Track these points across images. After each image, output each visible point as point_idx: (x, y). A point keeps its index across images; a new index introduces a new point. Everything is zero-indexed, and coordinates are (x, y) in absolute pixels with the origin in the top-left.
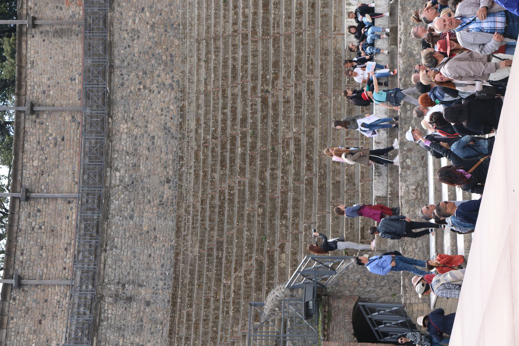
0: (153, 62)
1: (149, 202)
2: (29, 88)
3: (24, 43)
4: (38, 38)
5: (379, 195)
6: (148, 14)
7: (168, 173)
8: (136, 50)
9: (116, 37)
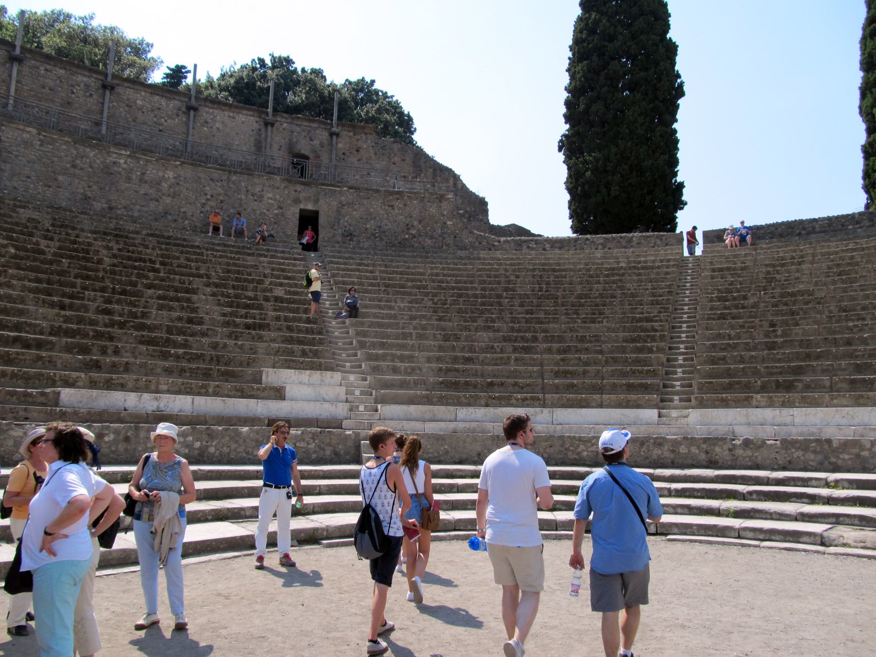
0: (232, 211)
1: (90, 187)
2: (211, 110)
3: (252, 113)
4: (256, 126)
5: (62, 396)
6: (276, 212)
7: (120, 209)
8: (243, 197)
9: (256, 180)
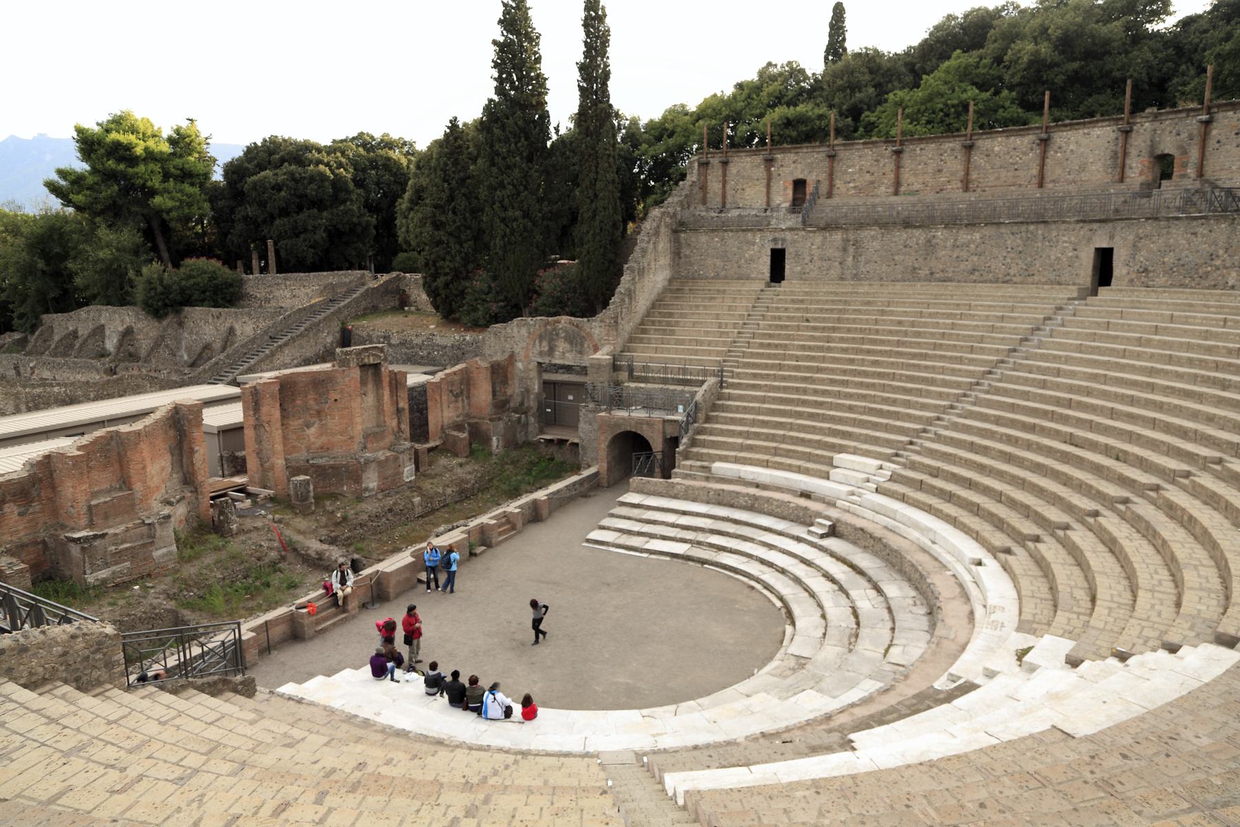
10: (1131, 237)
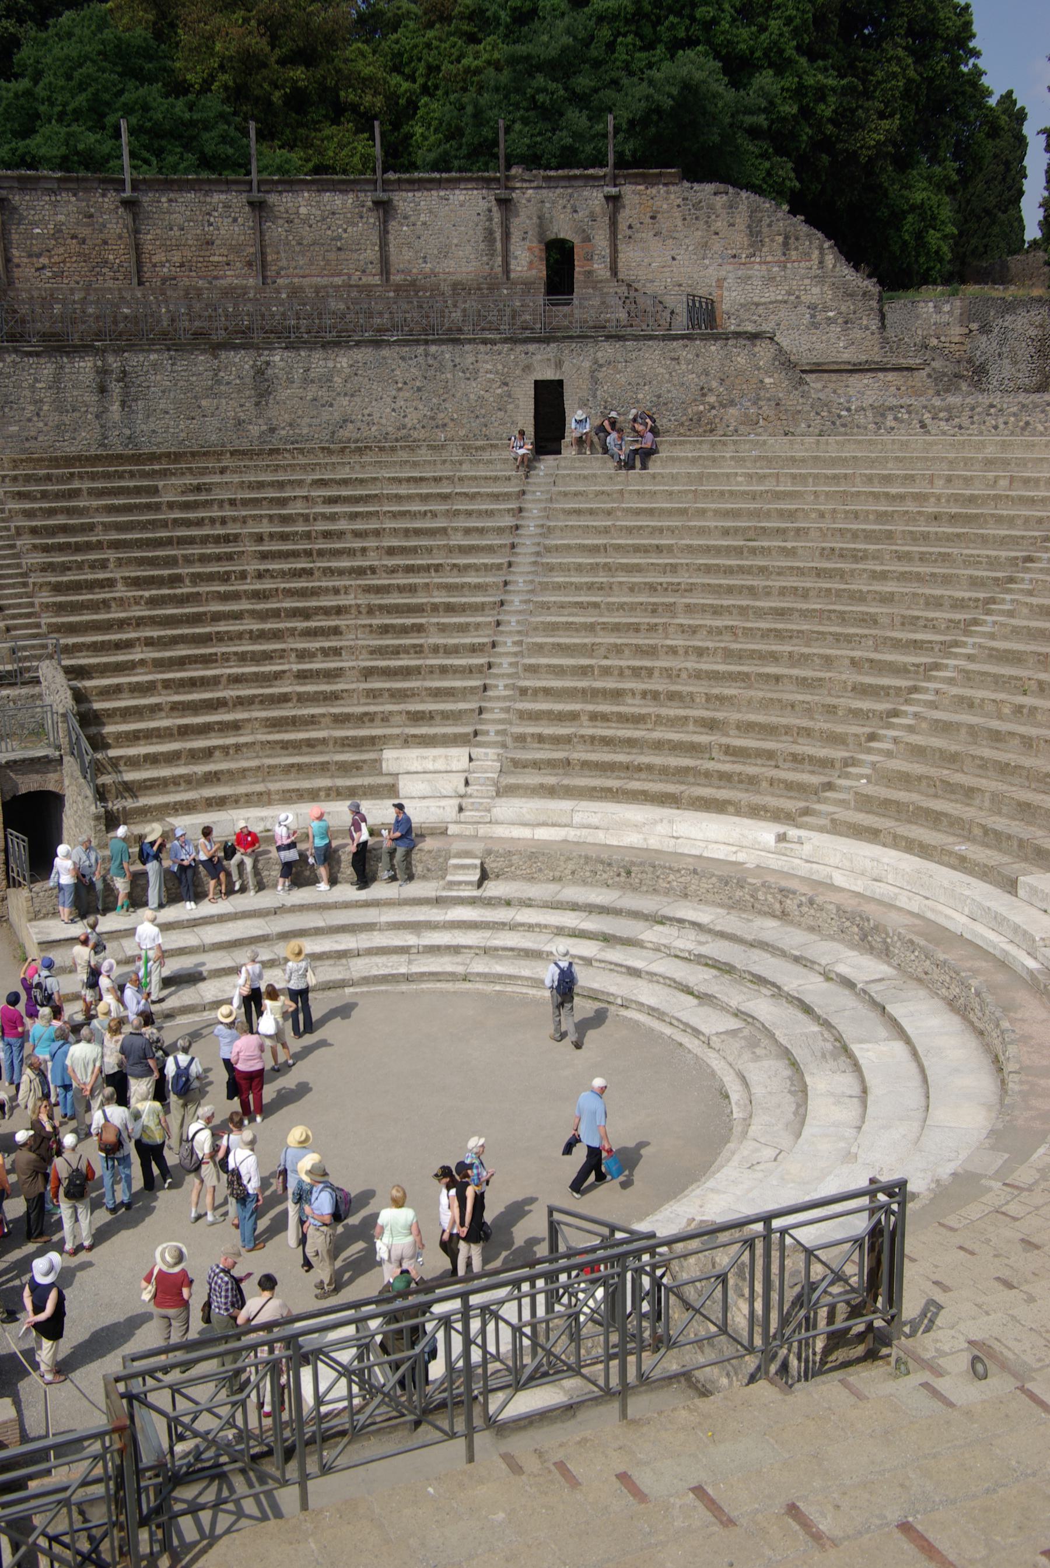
0: (434, 400)
1: (241, 406)
2: (410, 194)
6: (499, 391)
8: (449, 376)
10: (587, 364)
